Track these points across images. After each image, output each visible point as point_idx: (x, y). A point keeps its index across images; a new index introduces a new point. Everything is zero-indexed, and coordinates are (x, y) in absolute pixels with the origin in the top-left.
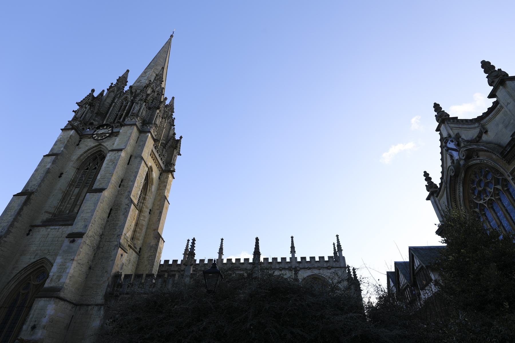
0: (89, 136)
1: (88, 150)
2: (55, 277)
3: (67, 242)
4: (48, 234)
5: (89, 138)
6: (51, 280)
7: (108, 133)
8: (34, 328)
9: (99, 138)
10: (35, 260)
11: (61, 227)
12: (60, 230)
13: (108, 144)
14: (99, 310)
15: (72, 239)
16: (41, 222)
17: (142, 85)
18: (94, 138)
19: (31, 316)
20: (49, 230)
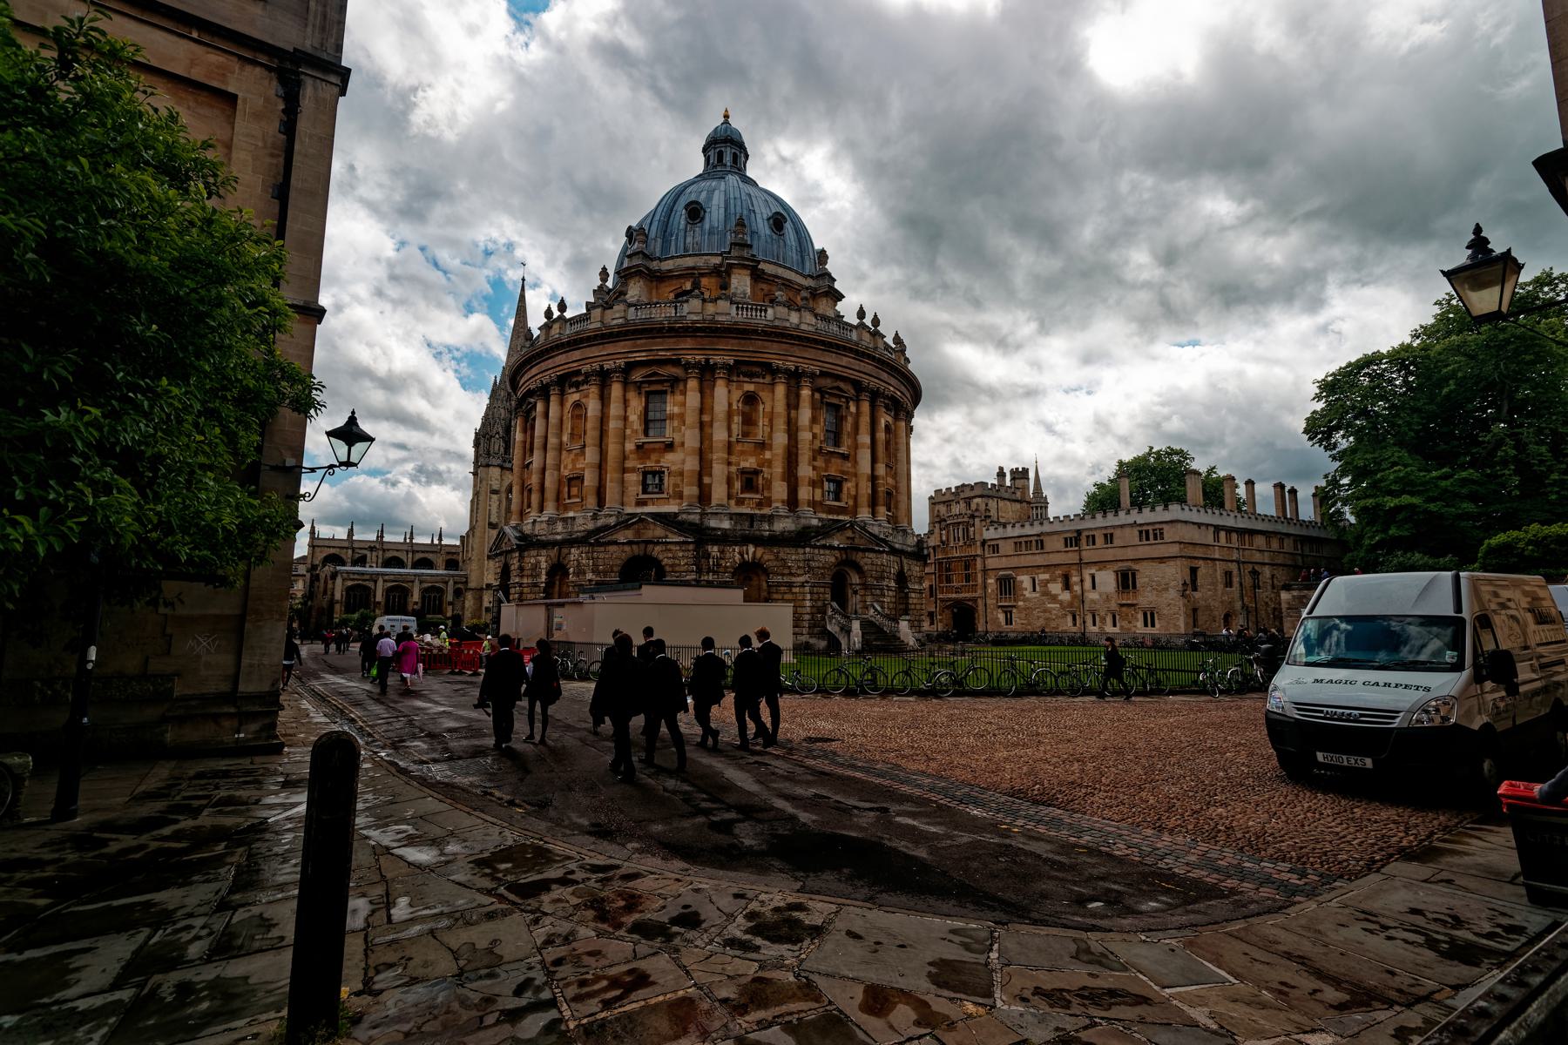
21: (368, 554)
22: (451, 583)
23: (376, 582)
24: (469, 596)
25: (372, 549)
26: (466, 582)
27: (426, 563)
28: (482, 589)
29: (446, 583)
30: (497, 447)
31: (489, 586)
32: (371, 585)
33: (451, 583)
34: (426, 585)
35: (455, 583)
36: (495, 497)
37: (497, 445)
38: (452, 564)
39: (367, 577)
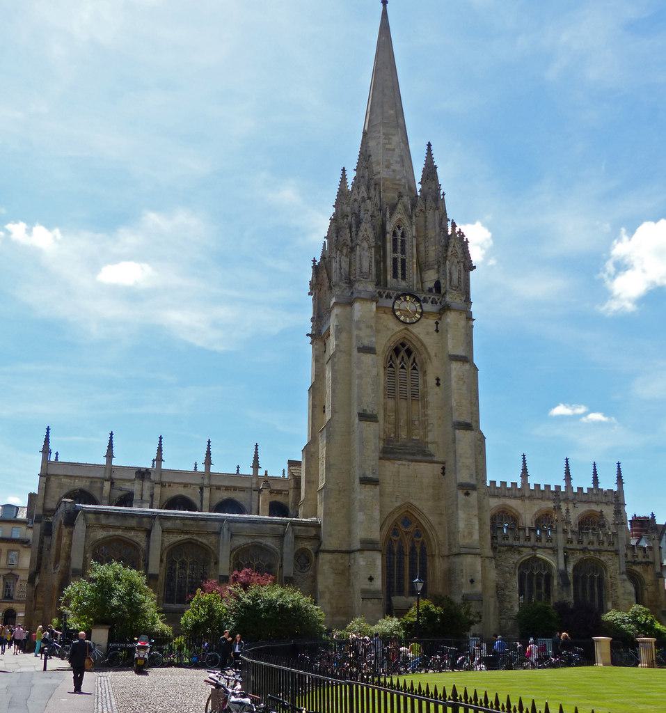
0: (387, 311)
1: (392, 336)
2: (466, 534)
3: (461, 495)
4: (399, 472)
5: (386, 313)
6: (464, 536)
7: (416, 312)
8: (472, 581)
9: (408, 322)
10: (398, 504)
11: (410, 463)
12: (411, 467)
13: (423, 331)
14: (491, 562)
15: (465, 491)
16: (381, 453)
17: (400, 180)
18: (397, 318)
19: (464, 571)
20: (396, 465)
21: (136, 487)
22: (290, 537)
23: (148, 533)
24: (325, 563)
25: (142, 474)
26: (317, 538)
27: (229, 505)
28: (349, 552)
29: (281, 537)
30: (366, 264)
31: (368, 545)
32: (139, 538)
33: (290, 537)
34: (241, 541)
35: (296, 537)
36: (368, 359)
37: (365, 258)
38: (277, 509)
39: (133, 523)
